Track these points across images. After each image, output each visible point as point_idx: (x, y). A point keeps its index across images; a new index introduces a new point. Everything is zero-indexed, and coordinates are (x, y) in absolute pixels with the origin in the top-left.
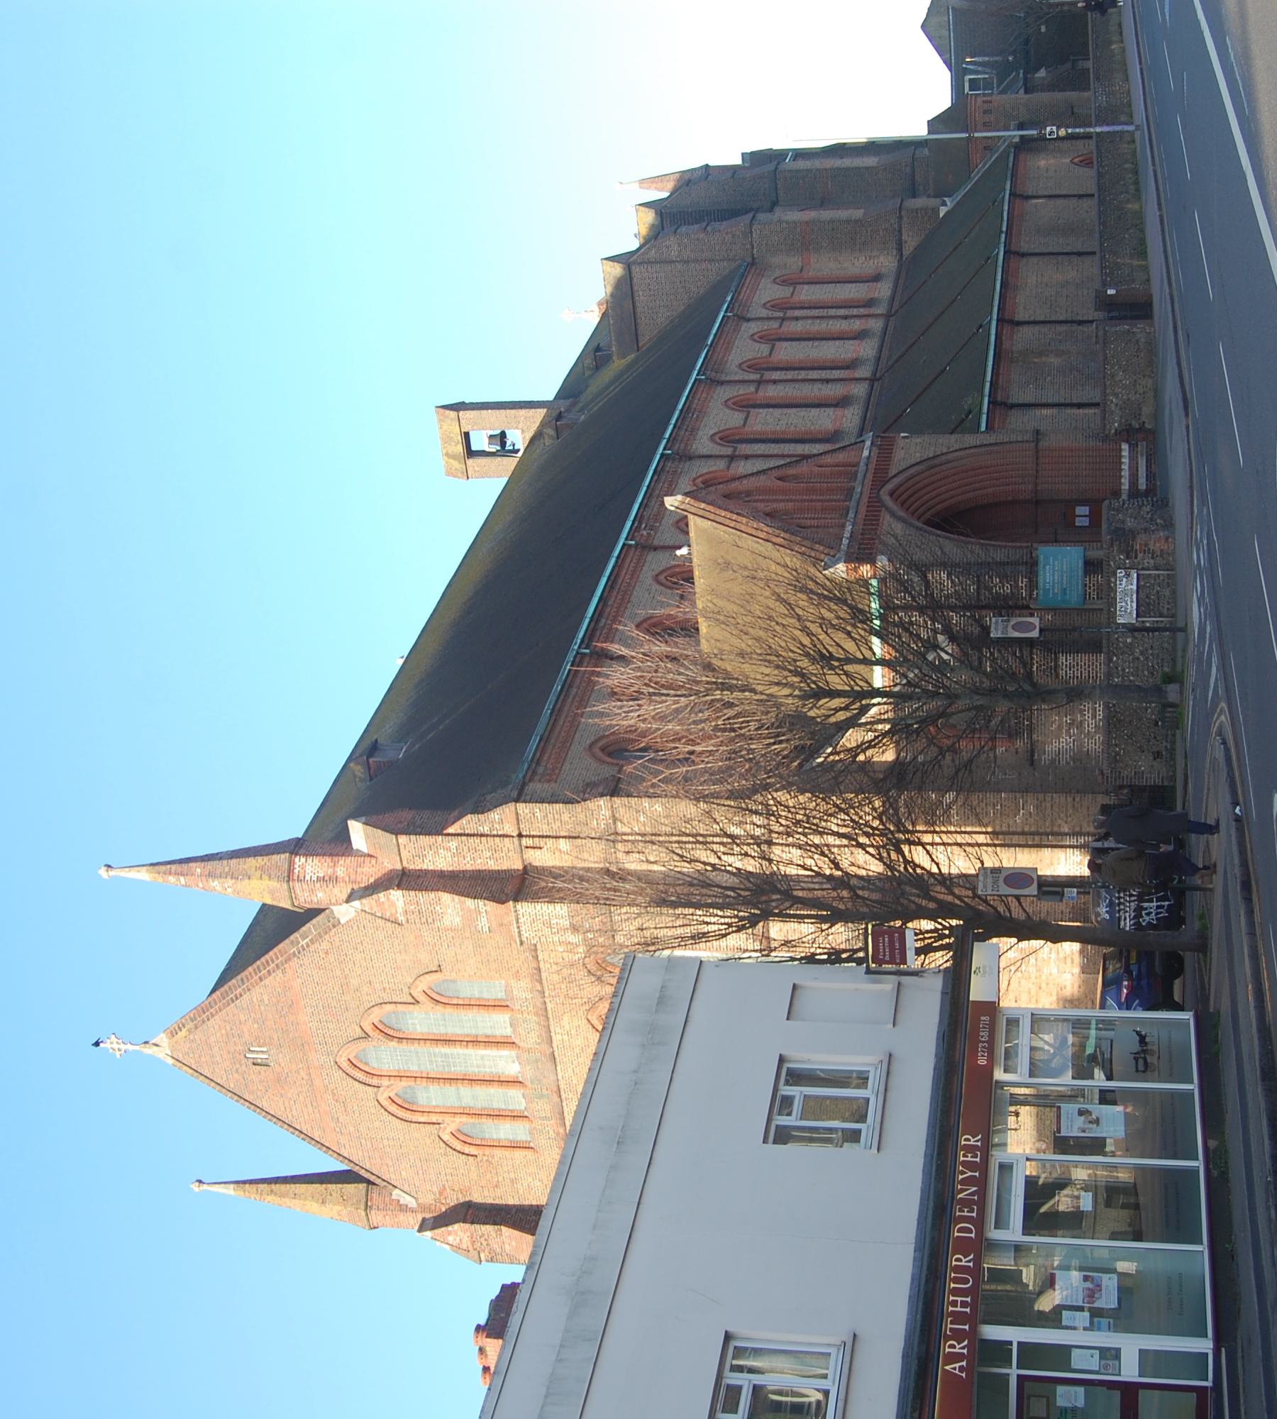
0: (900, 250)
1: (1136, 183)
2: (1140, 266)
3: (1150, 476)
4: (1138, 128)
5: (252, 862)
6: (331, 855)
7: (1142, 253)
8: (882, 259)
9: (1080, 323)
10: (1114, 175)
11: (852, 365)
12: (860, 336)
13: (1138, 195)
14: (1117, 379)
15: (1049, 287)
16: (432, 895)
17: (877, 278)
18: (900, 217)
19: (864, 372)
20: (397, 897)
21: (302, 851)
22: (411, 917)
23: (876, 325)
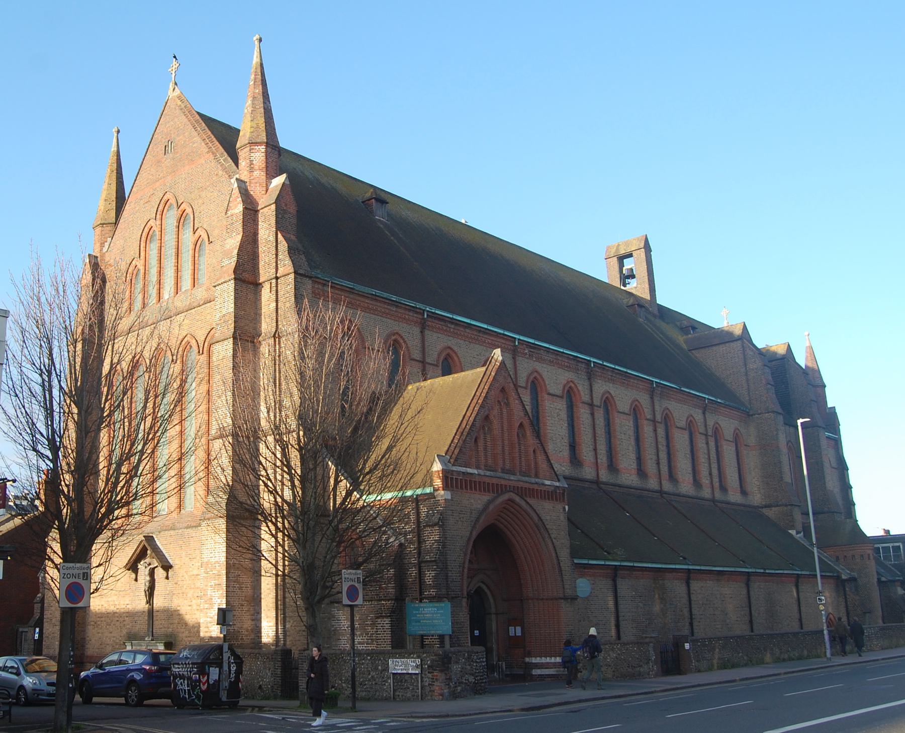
0: (766, 506)
1: (791, 659)
2: (713, 665)
4: (830, 659)
5: (261, 121)
6: (267, 167)
7: (724, 666)
8: (759, 495)
9: (691, 624)
10: (798, 644)
11: (672, 477)
12: (697, 483)
13: (778, 660)
14: (611, 653)
15: (721, 604)
16: (241, 229)
17: (744, 492)
18: (786, 506)
19: (667, 486)
20: (238, 208)
21: (269, 150)
22: (229, 219)
23: (706, 493)
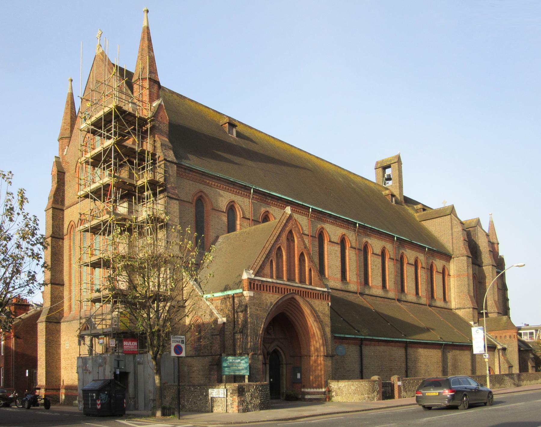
3: (311, 400)
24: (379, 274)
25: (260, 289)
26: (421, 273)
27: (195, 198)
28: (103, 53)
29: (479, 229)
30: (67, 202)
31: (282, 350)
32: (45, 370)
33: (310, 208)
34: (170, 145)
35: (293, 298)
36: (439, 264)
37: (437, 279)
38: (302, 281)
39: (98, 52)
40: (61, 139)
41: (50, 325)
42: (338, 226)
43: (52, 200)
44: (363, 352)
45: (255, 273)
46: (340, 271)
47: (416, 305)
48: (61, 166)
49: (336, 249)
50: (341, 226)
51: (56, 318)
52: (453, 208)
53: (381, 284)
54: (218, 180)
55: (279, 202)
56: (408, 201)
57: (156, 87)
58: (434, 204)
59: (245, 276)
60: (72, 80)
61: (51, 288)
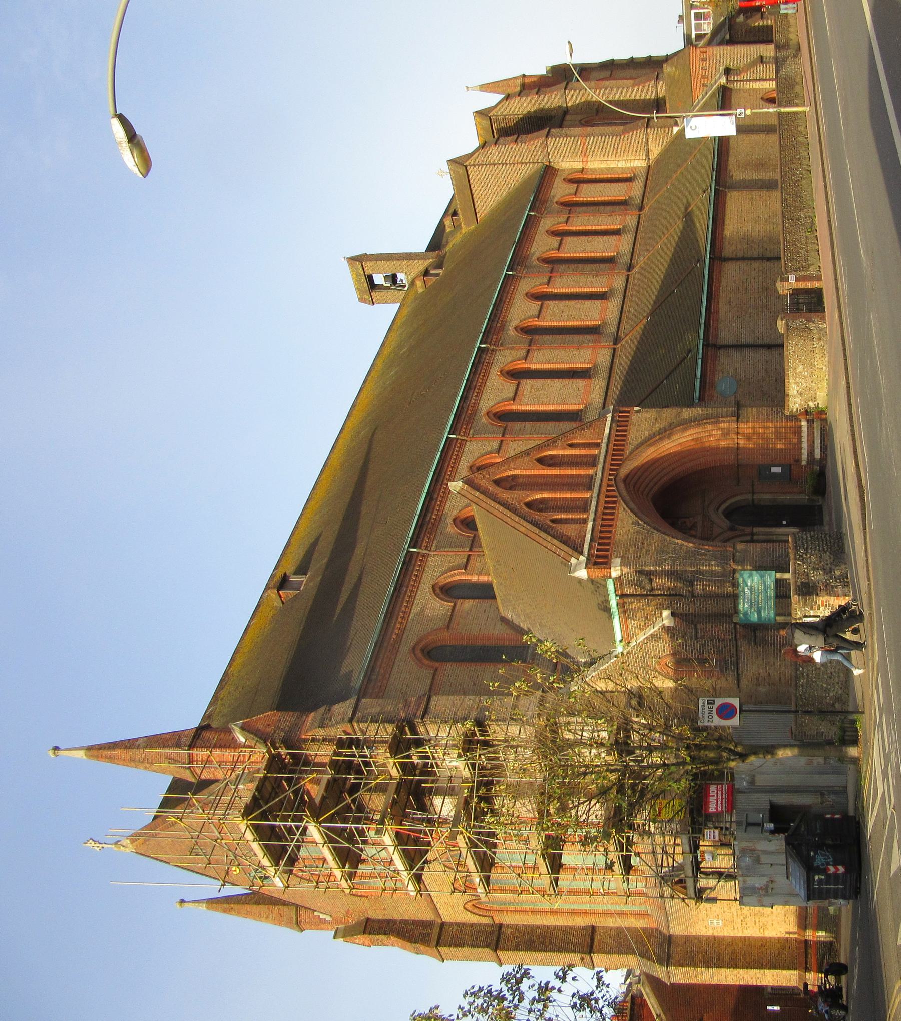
24: (579, 306)
25: (608, 544)
26: (580, 222)
27: (427, 662)
28: (134, 838)
29: (494, 112)
30: (426, 915)
31: (725, 502)
32: (767, 971)
33: (448, 438)
34: (322, 710)
35: (625, 481)
36: (560, 191)
37: (589, 193)
38: (592, 462)
39: (128, 848)
40: (299, 926)
41: (675, 957)
42: (484, 384)
43: (422, 948)
44: (731, 343)
45: (576, 554)
46: (571, 381)
47: (639, 236)
48: (353, 926)
49: (528, 388)
50: (486, 377)
51: (661, 944)
52: (452, 162)
53: (598, 303)
54: (391, 617)
55: (435, 496)
56: (436, 244)
57: (207, 735)
58: (441, 192)
59: (582, 573)
60: (182, 901)
61: (599, 952)
